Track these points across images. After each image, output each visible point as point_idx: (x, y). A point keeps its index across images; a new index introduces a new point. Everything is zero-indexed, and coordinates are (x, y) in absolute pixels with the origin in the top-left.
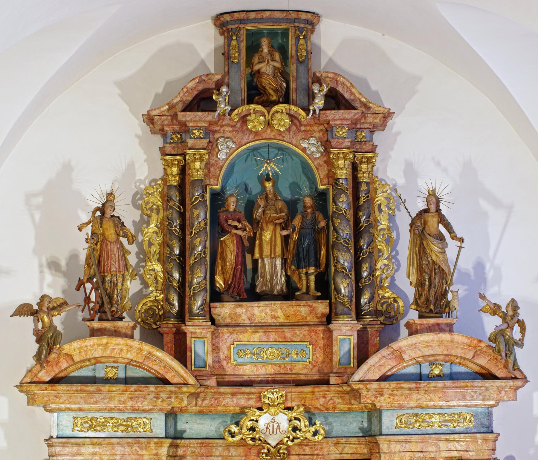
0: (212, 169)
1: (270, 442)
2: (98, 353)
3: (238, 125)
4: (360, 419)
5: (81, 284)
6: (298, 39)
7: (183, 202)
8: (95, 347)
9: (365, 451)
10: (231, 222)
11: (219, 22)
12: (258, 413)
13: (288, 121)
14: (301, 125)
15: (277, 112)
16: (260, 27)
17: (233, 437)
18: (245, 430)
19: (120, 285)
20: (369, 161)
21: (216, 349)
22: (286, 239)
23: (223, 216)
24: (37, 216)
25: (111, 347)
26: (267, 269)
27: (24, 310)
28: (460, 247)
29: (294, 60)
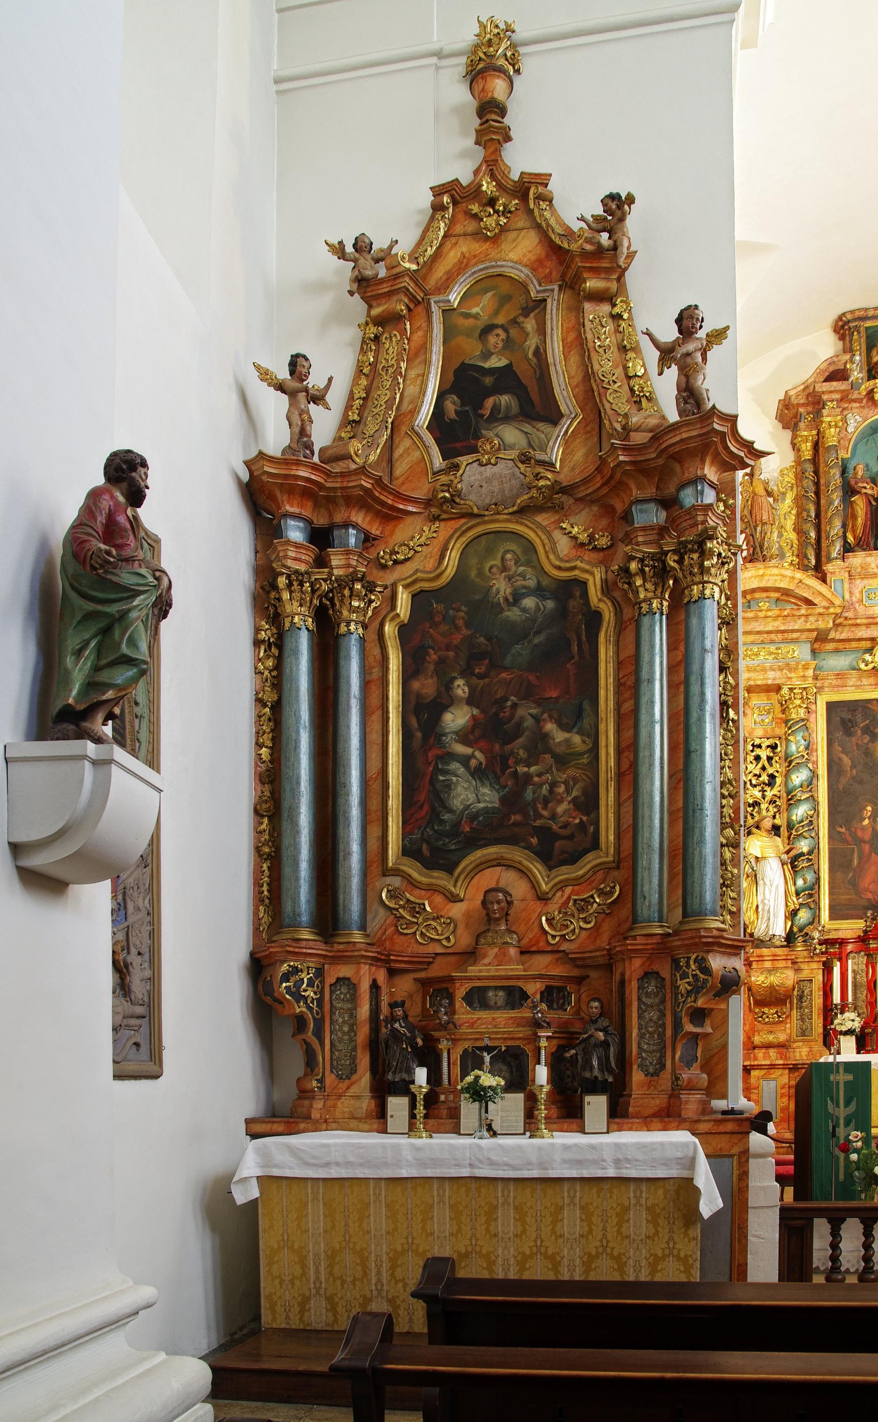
10: (860, 485)
17: (866, 665)
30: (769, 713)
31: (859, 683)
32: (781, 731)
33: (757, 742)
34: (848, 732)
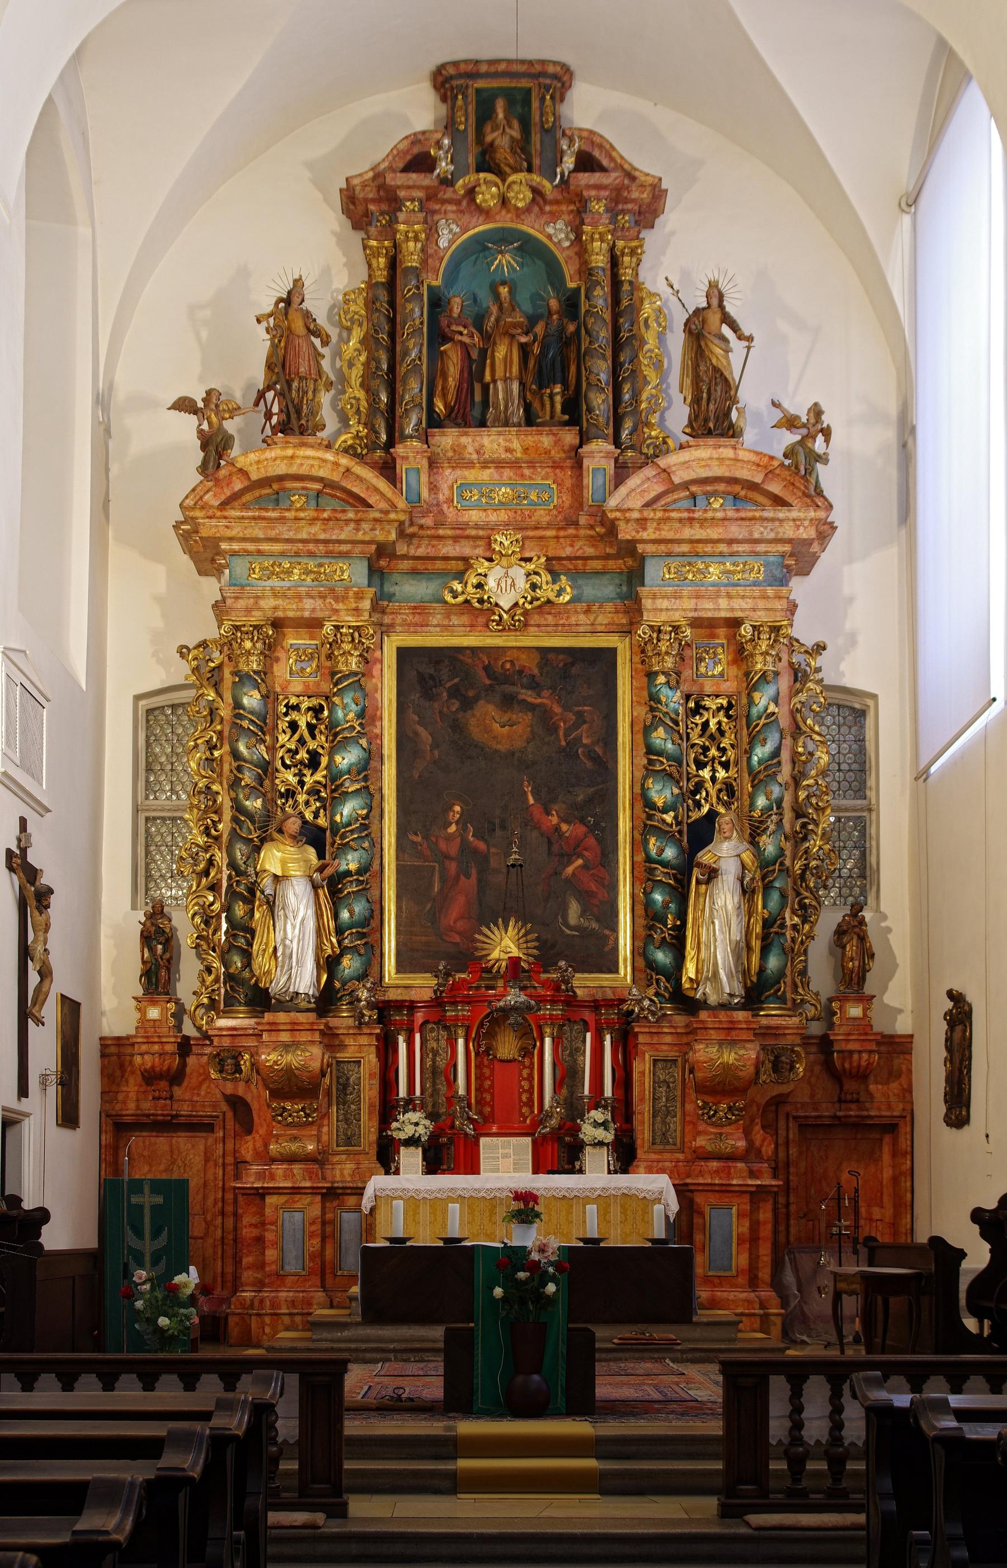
0: (430, 261)
1: (501, 604)
2: (282, 469)
3: (464, 203)
4: (617, 581)
5: (261, 395)
6: (543, 99)
7: (392, 304)
8: (278, 462)
9: (624, 621)
10: (454, 328)
11: (440, 79)
12: (486, 564)
13: (529, 195)
14: (545, 202)
15: (514, 182)
16: (495, 84)
18: (470, 589)
19: (310, 393)
20: (633, 252)
21: (433, 488)
22: (525, 350)
23: (444, 322)
24: (204, 335)
25: (298, 461)
26: (501, 397)
27: (184, 405)
28: (749, 348)
29: (538, 128)
30: (312, 659)
31: (446, 622)
32: (326, 687)
33: (293, 701)
34: (428, 695)
